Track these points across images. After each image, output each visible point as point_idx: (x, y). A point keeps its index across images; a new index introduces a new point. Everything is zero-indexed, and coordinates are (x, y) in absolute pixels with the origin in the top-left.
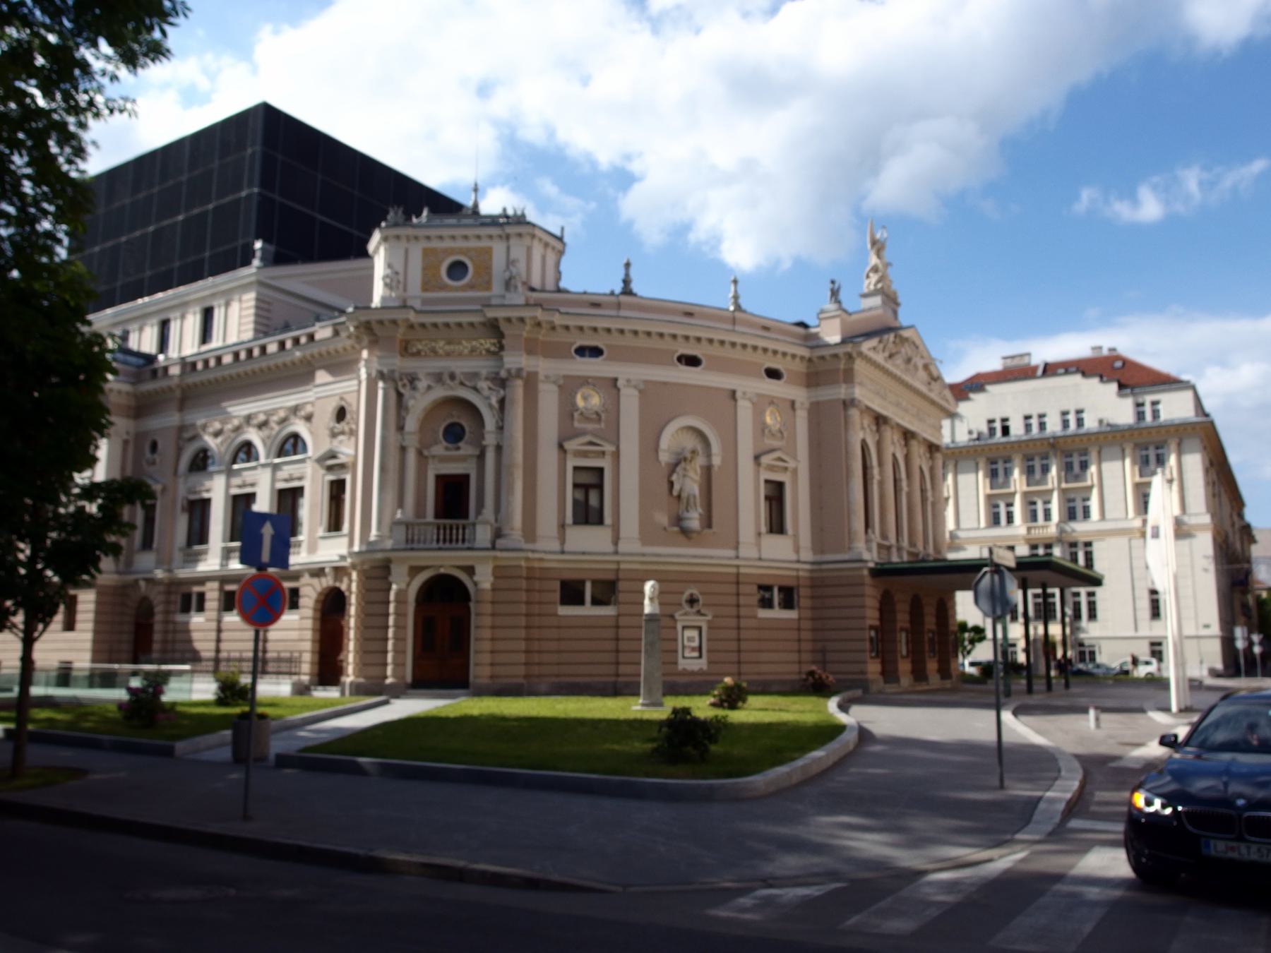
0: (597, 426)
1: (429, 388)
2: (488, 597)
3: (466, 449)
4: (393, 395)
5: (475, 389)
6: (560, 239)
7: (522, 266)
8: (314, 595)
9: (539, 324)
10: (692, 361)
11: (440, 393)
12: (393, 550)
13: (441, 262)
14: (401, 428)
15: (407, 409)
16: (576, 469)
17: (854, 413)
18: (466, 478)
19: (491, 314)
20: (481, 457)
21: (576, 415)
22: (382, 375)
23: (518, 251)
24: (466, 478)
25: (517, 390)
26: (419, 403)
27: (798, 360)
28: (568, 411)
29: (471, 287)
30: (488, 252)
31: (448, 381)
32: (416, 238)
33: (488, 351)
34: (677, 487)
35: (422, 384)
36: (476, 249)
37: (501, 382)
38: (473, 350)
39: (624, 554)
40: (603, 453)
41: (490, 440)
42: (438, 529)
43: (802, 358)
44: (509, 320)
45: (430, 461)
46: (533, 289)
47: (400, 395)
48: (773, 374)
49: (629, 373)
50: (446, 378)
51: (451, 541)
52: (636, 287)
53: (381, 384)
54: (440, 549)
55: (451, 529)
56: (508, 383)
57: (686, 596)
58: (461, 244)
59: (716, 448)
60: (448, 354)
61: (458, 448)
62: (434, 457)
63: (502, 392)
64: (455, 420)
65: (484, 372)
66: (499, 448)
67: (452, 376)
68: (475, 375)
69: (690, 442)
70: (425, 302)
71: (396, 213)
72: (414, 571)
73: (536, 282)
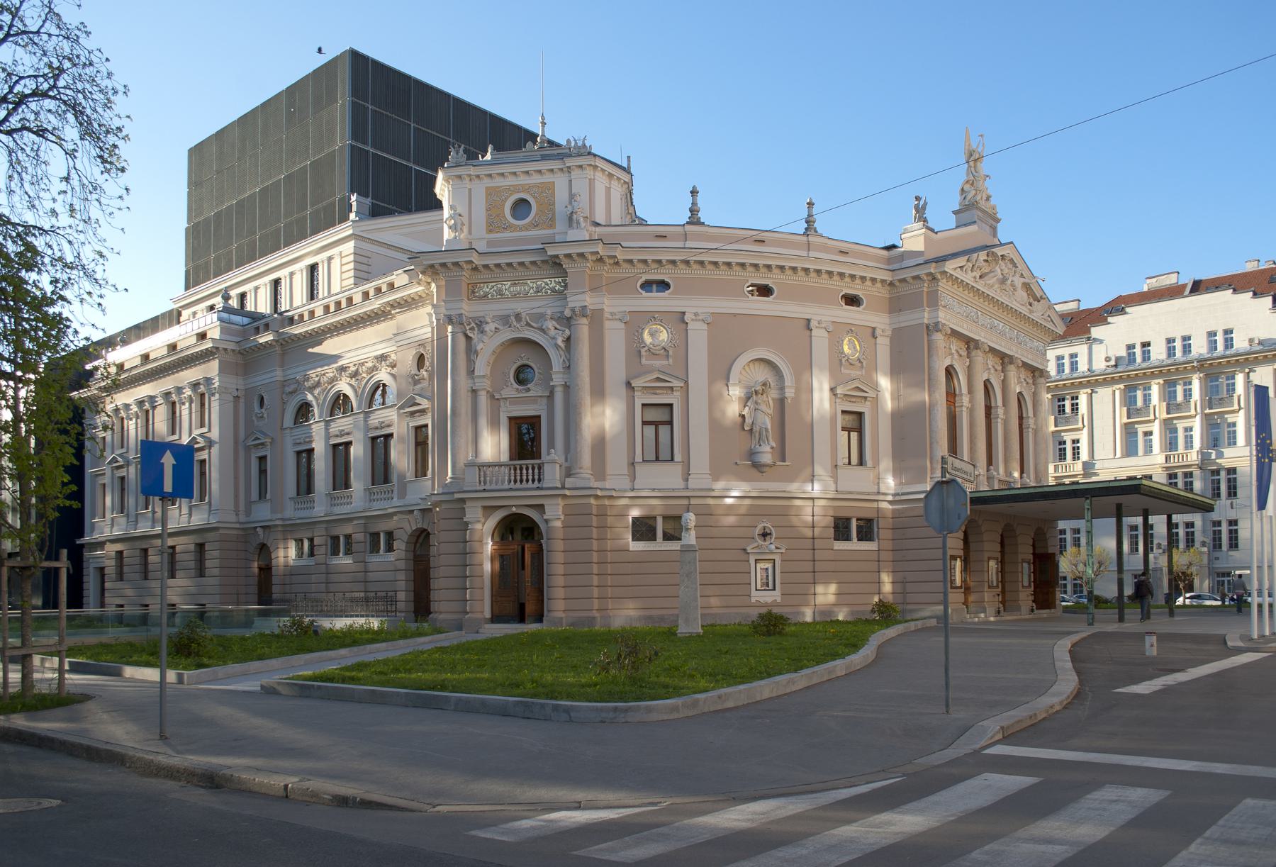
0: (665, 362)
2: (560, 534)
3: (535, 389)
4: (462, 339)
5: (543, 331)
6: (627, 170)
7: (583, 200)
8: (405, 538)
9: (601, 260)
10: (765, 291)
11: (508, 335)
13: (504, 201)
14: (471, 372)
15: (476, 353)
16: (643, 405)
17: (939, 338)
18: (539, 417)
19: (551, 251)
20: (551, 397)
21: (643, 351)
22: (450, 320)
23: (580, 186)
24: (539, 417)
25: (583, 329)
26: (487, 346)
27: (879, 285)
28: (636, 350)
29: (535, 225)
33: (553, 290)
34: (748, 421)
35: (489, 328)
36: (537, 186)
37: (567, 322)
39: (694, 490)
40: (672, 388)
41: (558, 380)
43: (883, 281)
44: (569, 256)
45: (502, 403)
46: (597, 224)
47: (468, 338)
48: (852, 300)
49: (696, 306)
52: (703, 216)
53: (450, 328)
54: (511, 489)
55: (521, 469)
56: (573, 322)
57: (758, 530)
58: (523, 180)
59: (789, 381)
61: (529, 390)
63: (567, 332)
64: (525, 362)
65: (549, 312)
66: (566, 387)
67: (518, 317)
68: (541, 316)
69: (762, 374)
70: (490, 243)
71: (457, 153)
73: (600, 218)
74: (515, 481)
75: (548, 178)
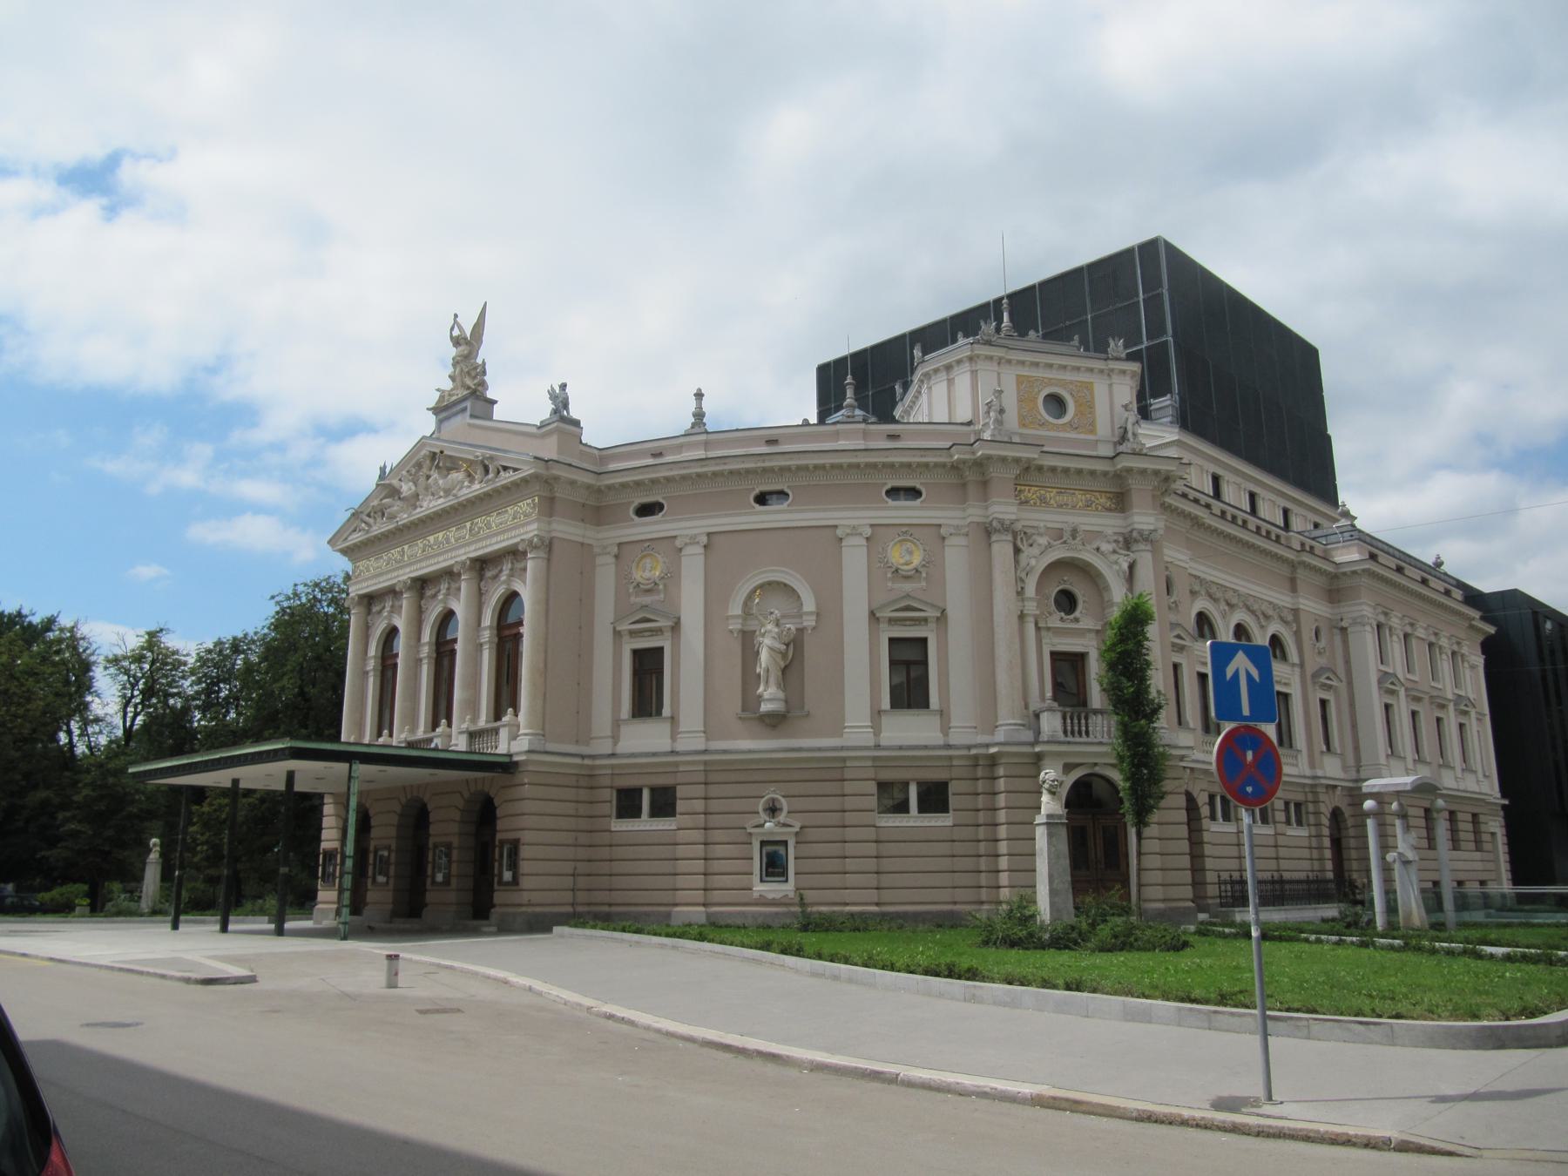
1: (1050, 546)
12: (529, 752)
14: (1020, 593)
29: (1071, 426)
30: (1089, 387)
31: (1070, 541)
32: (1009, 362)
42: (1064, 718)
47: (1017, 551)
50: (1066, 536)
51: (1073, 733)
62: (1049, 629)
65: (1110, 531)
72: (1068, 768)
74: (1065, 732)
75: (1083, 377)
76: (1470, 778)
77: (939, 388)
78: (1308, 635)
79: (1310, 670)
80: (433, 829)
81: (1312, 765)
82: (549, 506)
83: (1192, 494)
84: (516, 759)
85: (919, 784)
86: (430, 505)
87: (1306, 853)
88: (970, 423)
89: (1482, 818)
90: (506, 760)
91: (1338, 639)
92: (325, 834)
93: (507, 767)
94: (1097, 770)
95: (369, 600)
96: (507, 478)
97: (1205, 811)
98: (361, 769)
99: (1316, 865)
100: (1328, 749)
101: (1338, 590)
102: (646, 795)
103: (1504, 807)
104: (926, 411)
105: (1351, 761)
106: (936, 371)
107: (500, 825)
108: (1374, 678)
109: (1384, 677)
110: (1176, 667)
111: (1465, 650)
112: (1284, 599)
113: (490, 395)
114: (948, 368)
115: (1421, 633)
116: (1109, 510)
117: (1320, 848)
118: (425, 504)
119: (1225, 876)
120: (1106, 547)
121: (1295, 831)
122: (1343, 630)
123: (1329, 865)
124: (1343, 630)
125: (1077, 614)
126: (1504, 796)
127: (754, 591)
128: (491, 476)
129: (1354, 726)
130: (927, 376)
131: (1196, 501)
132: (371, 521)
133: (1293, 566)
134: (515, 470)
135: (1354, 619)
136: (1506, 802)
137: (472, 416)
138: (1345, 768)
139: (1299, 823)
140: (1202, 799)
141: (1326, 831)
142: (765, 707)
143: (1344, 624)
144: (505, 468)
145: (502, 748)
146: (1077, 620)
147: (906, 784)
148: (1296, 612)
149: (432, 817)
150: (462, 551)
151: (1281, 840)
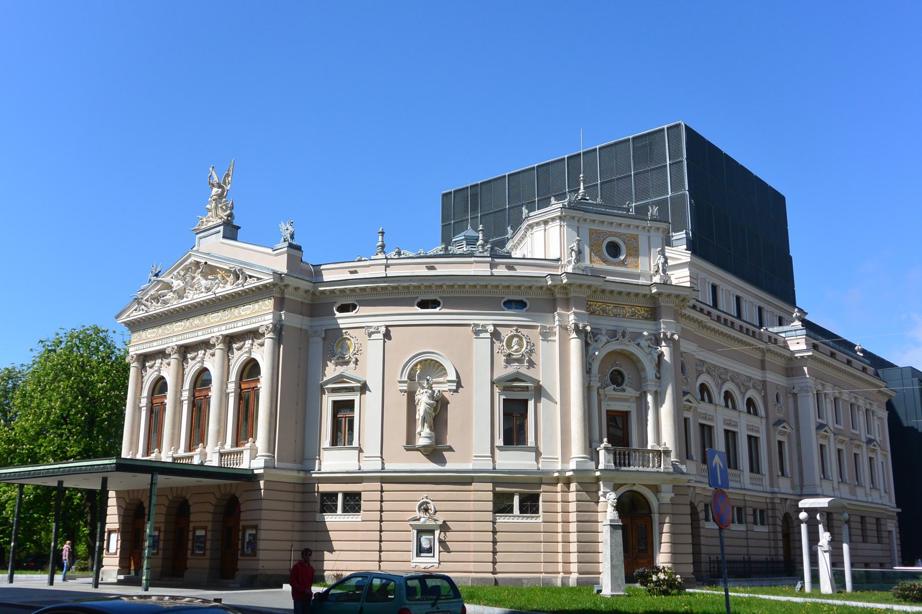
3: (630, 392)
5: (638, 344)
11: (614, 346)
30: (635, 238)
35: (604, 339)
38: (633, 315)
55: (624, 455)
60: (615, 316)
74: (615, 463)
76: (875, 494)
77: (538, 232)
78: (771, 398)
79: (771, 422)
80: (192, 518)
81: (772, 485)
82: (280, 304)
83: (699, 305)
84: (256, 472)
85: (521, 495)
86: (193, 297)
87: (766, 543)
88: (559, 260)
89: (883, 521)
90: (250, 473)
91: (791, 400)
92: (109, 519)
93: (249, 477)
94: (635, 488)
95: (144, 358)
96: (251, 284)
97: (702, 515)
98: (161, 479)
99: (773, 551)
100: (783, 475)
101: (792, 368)
102: (340, 496)
103: (898, 513)
104: (529, 249)
105: (797, 482)
106: (538, 224)
107: (243, 516)
108: (813, 427)
109: (820, 427)
110: (686, 420)
111: (875, 408)
112: (757, 374)
113: (235, 223)
114: (546, 222)
115: (845, 397)
116: (646, 319)
117: (775, 540)
118: (190, 297)
119: (714, 558)
120: (644, 343)
121: (759, 528)
122: (795, 395)
123: (781, 551)
124: (795, 395)
125: (624, 386)
126: (899, 504)
127: (416, 365)
128: (240, 281)
129: (800, 459)
130: (531, 226)
131: (701, 311)
132: (149, 304)
133: (762, 350)
134: (259, 279)
135: (802, 388)
136: (900, 510)
137: (224, 237)
138: (793, 487)
139: (762, 523)
140: (700, 508)
141: (779, 529)
142: (421, 441)
143: (795, 391)
144: (251, 277)
145: (245, 465)
146: (624, 390)
147: (511, 495)
148: (764, 383)
149: (192, 509)
150: (216, 329)
151: (750, 535)
